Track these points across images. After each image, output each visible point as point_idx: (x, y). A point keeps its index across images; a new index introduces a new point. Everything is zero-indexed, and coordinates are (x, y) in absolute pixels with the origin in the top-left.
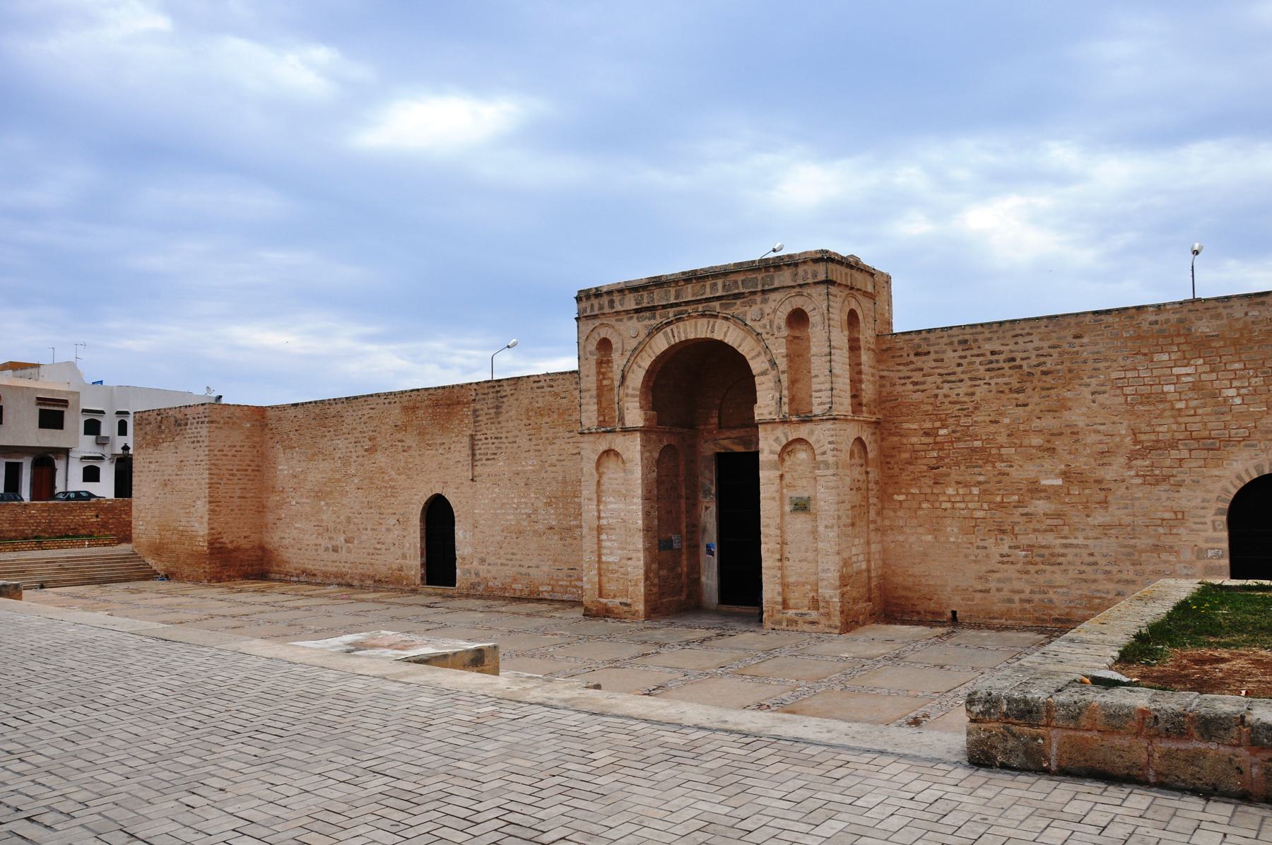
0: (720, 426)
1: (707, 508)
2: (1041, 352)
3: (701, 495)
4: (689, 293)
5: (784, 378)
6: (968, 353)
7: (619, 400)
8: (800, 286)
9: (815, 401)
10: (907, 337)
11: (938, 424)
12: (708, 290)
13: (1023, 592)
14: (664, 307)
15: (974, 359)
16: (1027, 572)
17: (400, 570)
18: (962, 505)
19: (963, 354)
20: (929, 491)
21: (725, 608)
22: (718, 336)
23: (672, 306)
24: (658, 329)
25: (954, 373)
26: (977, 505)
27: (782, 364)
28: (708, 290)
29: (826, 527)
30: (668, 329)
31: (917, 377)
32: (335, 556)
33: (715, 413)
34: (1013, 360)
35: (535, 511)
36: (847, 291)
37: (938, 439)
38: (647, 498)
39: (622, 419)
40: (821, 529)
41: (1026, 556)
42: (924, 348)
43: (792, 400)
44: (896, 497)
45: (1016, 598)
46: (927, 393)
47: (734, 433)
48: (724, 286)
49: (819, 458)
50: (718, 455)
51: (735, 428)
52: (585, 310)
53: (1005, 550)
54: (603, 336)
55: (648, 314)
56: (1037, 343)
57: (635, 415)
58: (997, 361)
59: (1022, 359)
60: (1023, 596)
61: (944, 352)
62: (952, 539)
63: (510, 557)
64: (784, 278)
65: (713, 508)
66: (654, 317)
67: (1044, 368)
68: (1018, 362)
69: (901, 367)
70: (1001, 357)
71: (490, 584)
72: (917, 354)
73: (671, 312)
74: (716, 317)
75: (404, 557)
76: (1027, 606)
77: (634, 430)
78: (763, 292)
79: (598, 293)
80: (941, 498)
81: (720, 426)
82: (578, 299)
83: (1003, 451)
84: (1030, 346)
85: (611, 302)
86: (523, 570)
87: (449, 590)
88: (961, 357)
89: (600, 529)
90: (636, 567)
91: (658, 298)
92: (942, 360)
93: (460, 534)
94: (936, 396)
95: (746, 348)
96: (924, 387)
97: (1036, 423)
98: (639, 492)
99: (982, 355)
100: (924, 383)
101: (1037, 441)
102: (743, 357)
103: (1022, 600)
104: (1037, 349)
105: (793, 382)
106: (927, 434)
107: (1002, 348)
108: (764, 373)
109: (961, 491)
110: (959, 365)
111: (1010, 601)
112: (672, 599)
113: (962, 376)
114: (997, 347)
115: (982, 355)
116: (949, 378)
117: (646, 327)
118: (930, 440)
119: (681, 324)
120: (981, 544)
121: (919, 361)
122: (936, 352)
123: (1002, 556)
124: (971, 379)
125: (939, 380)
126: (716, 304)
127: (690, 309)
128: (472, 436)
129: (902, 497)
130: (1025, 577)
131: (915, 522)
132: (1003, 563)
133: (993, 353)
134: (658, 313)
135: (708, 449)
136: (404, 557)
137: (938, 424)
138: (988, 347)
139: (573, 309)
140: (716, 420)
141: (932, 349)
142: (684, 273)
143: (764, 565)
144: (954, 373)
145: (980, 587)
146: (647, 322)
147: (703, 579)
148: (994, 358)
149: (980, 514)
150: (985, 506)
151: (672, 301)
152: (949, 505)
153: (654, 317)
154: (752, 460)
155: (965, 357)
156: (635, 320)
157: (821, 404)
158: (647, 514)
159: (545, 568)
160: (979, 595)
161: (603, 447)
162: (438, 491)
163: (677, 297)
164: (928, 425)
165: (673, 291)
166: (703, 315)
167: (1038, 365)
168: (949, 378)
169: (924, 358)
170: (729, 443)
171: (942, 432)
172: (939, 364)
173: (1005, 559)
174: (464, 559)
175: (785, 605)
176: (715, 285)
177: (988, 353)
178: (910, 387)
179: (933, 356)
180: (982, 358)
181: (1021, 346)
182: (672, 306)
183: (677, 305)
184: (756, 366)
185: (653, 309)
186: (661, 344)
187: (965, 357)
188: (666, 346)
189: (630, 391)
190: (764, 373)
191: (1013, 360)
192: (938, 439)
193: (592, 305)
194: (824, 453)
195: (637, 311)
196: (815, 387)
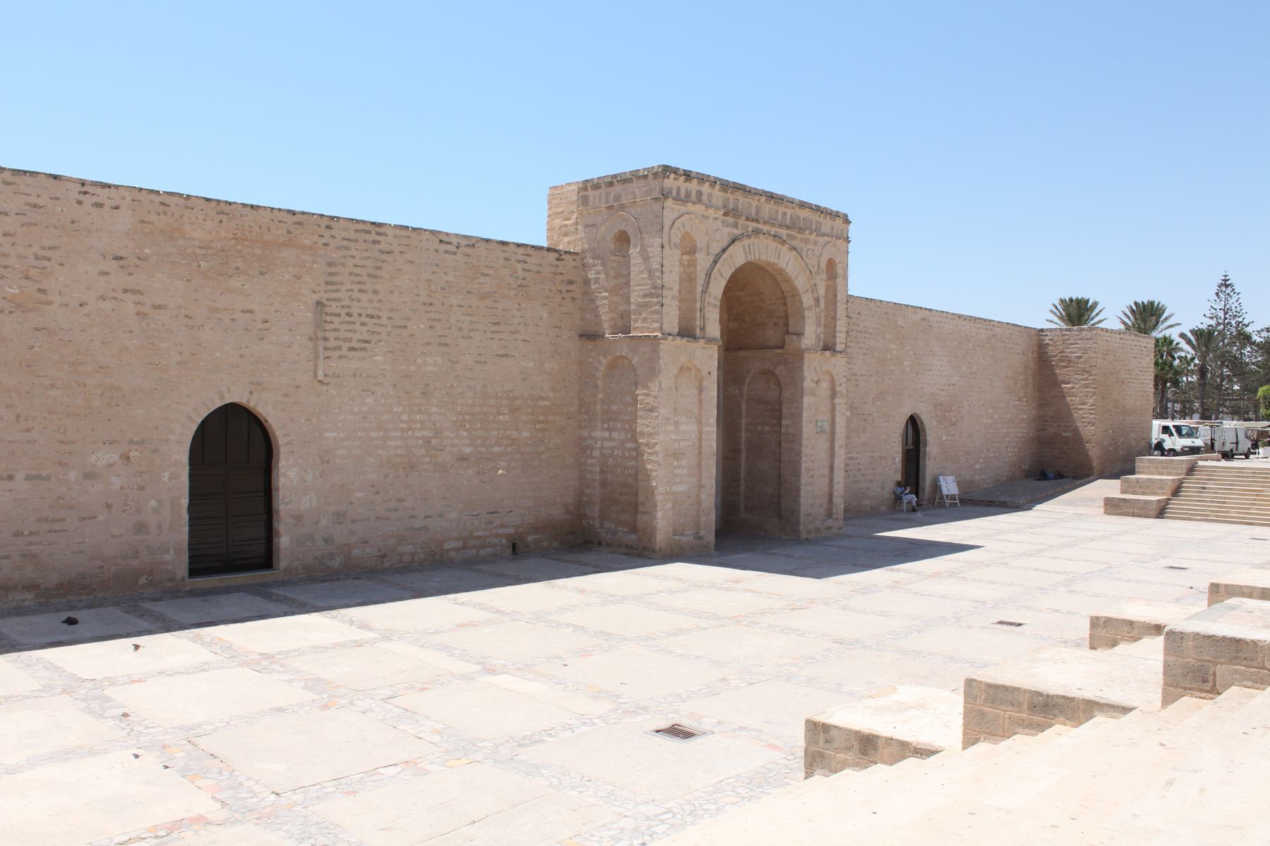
9: (838, 341)
35: (438, 433)
39: (702, 329)
73: (752, 225)
74: (783, 243)
86: (418, 523)
108: (810, 308)
127: (765, 228)
128: (319, 303)
146: (729, 230)
153: (736, 226)
159: (453, 515)
162: (237, 396)
174: (298, 518)
184: (807, 300)
189: (711, 300)
190: (810, 308)
193: (679, 189)
196: (838, 329)
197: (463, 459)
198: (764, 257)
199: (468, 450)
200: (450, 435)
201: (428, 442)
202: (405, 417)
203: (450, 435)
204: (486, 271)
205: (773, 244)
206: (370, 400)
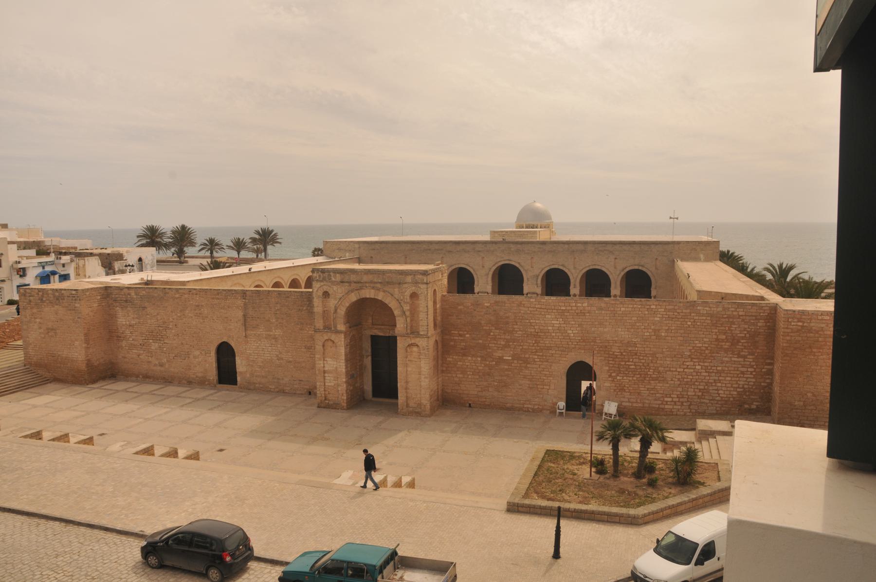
4: (365, 278)
5: (408, 320)
7: (334, 319)
22: (380, 298)
24: (352, 291)
27: (408, 313)
32: (162, 369)
38: (347, 360)
39: (335, 327)
43: (412, 326)
57: (341, 327)
77: (341, 332)
89: (324, 372)
90: (343, 388)
95: (393, 304)
97: (503, 337)
98: (343, 358)
101: (503, 343)
105: (411, 321)
112: (356, 401)
126: (378, 285)
135: (369, 333)
140: (370, 321)
147: (365, 387)
158: (347, 367)
161: (326, 338)
166: (373, 288)
175: (407, 406)
184: (396, 312)
185: (349, 282)
186: (353, 297)
197: (290, 362)
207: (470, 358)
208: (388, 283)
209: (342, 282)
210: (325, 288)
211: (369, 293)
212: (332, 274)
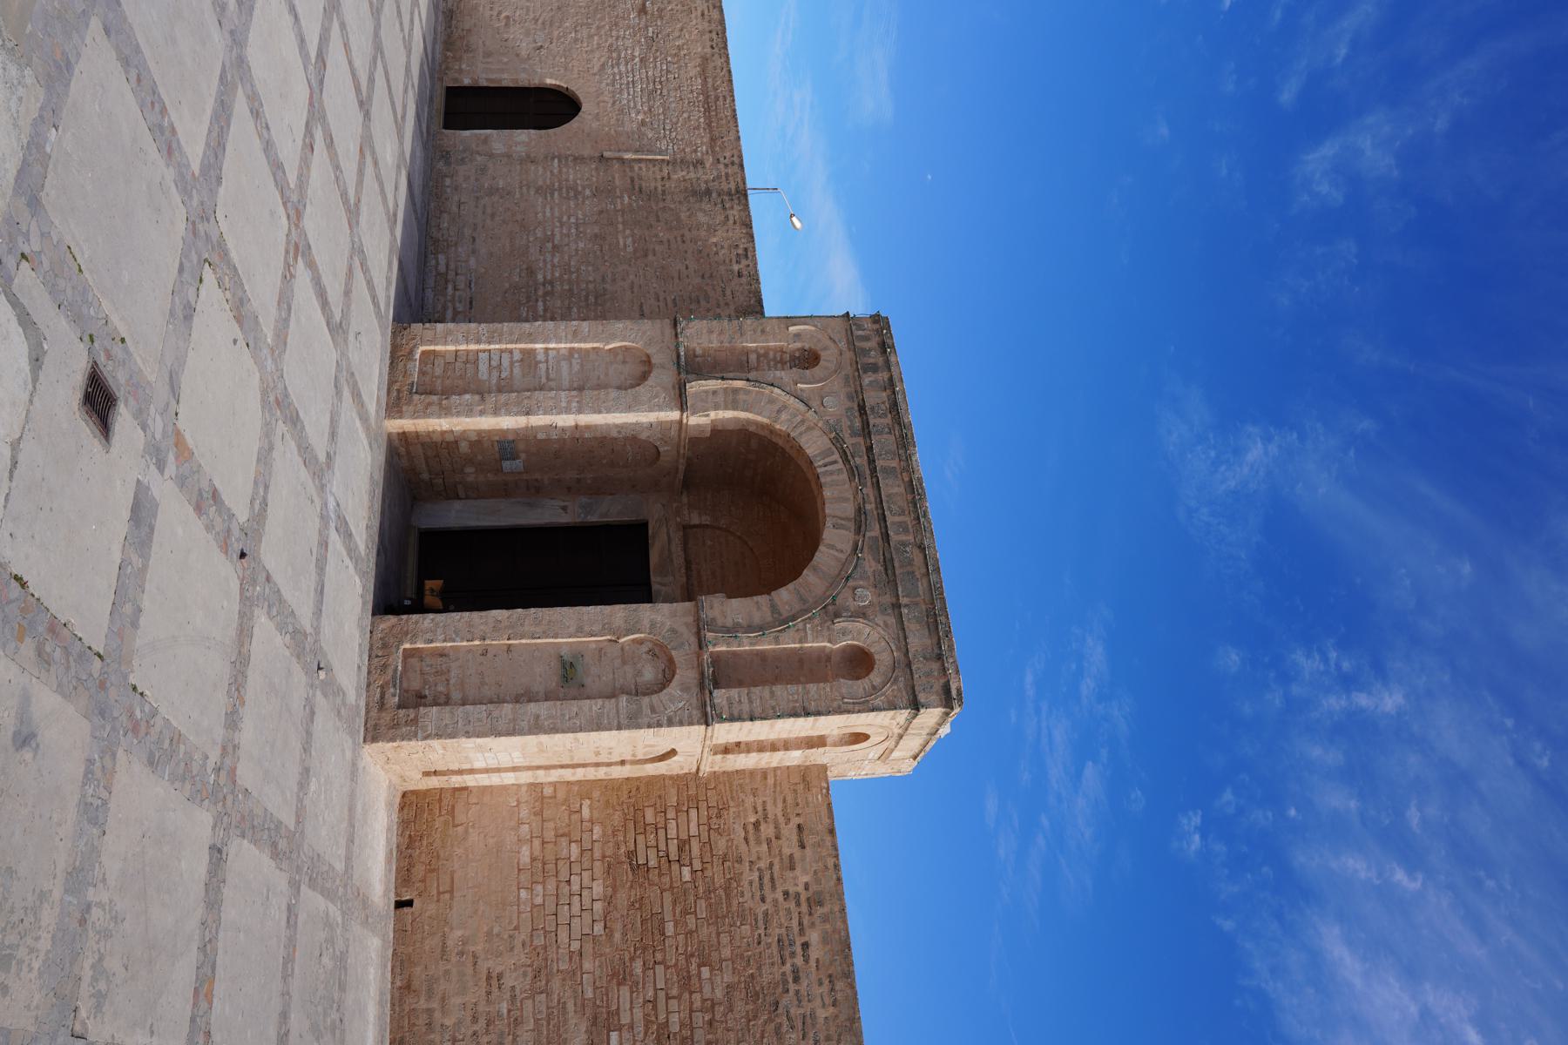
0: (686, 528)
1: (564, 508)
2: (809, 1021)
3: (584, 500)
4: (893, 488)
6: (804, 908)
8: (909, 665)
9: (734, 692)
10: (824, 812)
11: (697, 865)
12: (897, 519)
13: (443, 1012)
14: (870, 449)
15: (795, 916)
16: (475, 1020)
17: (468, 49)
18: (576, 909)
19: (803, 898)
20: (597, 855)
21: (413, 541)
22: (829, 534)
23: (871, 461)
25: (774, 887)
26: (576, 934)
28: (897, 519)
29: (538, 717)
30: (836, 456)
31: (767, 830)
33: (706, 520)
34: (796, 980)
36: (897, 731)
37: (675, 867)
40: (532, 708)
41: (499, 1015)
42: (810, 840)
44: (587, 803)
45: (435, 1005)
46: (743, 847)
47: (677, 549)
48: (904, 544)
49: (646, 700)
50: (645, 525)
51: (685, 550)
52: (860, 327)
53: (508, 981)
54: (823, 354)
55: (858, 424)
56: (822, 1014)
58: (793, 954)
59: (797, 992)
60: (437, 1015)
61: (805, 872)
62: (523, 894)
63: (489, 211)
64: (918, 640)
65: (564, 519)
66: (853, 435)
67: (785, 1028)
68: (792, 987)
69: (780, 805)
70: (799, 961)
71: (448, 181)
72: (799, 826)
73: (861, 461)
74: (858, 531)
75: (488, 54)
76: (422, 1020)
78: (897, 606)
79: (885, 347)
80: (586, 875)
81: (686, 528)
82: (876, 318)
83: (660, 969)
84: (818, 1002)
85: (874, 368)
86: (467, 232)
87: (439, 119)
88: (798, 895)
91: (883, 442)
92: (792, 868)
93: (523, 137)
94: (740, 860)
96: (752, 842)
99: (802, 931)
100: (759, 842)
102: (796, 573)
103: (430, 1011)
104: (813, 1015)
106: (683, 845)
107: (813, 963)
108: (774, 608)
109: (598, 906)
110: (786, 893)
111: (430, 994)
113: (768, 900)
114: (814, 953)
115: (802, 931)
116: (766, 880)
117: (838, 421)
118: (674, 855)
119: (845, 476)
120: (518, 943)
121: (789, 832)
122: (803, 859)
123: (500, 977)
124: (766, 914)
125: (762, 864)
126: (874, 531)
129: (586, 813)
130: (468, 1015)
131: (550, 835)
132: (489, 978)
133: (805, 946)
134: (860, 440)
135: (653, 511)
136: (488, 54)
137: (697, 865)
138: (814, 937)
139: (860, 309)
140: (695, 520)
141: (808, 851)
142: (920, 480)
143: (475, 615)
144: (774, 887)
145: (450, 943)
146: (845, 423)
147: (457, 505)
148: (799, 949)
149: (563, 936)
150: (575, 946)
151: (879, 463)
152: (576, 888)
153: (853, 435)
154: (639, 591)
155: (798, 904)
156: (849, 404)
157: (730, 704)
160: (435, 941)
162: (586, 107)
163: (884, 469)
164: (695, 847)
165: (894, 464)
166: (860, 511)
167: (789, 1019)
168: (766, 880)
169: (795, 838)
170: (663, 546)
171: (686, 871)
172: (787, 861)
173: (494, 982)
176: (906, 530)
177: (804, 939)
178: (753, 820)
179: (797, 853)
180: (796, 929)
181: (817, 991)
182: (871, 461)
183: (873, 471)
184: (785, 596)
185: (866, 430)
186: (814, 445)
187: (798, 904)
188: (810, 451)
190: (774, 608)
191: (796, 980)
192: (675, 867)
193: (867, 338)
194: (653, 710)
195: (862, 408)
196: (756, 690)
198: (827, 493)
199: (540, 277)
200: (556, 260)
201: (551, 239)
202: (573, 220)
203: (556, 260)
204: (728, 292)
205: (849, 509)
206: (588, 192)
207: (598, 889)
208: (888, 564)
209: (862, 408)
210: (829, 357)
211: (837, 497)
212: (883, 376)
